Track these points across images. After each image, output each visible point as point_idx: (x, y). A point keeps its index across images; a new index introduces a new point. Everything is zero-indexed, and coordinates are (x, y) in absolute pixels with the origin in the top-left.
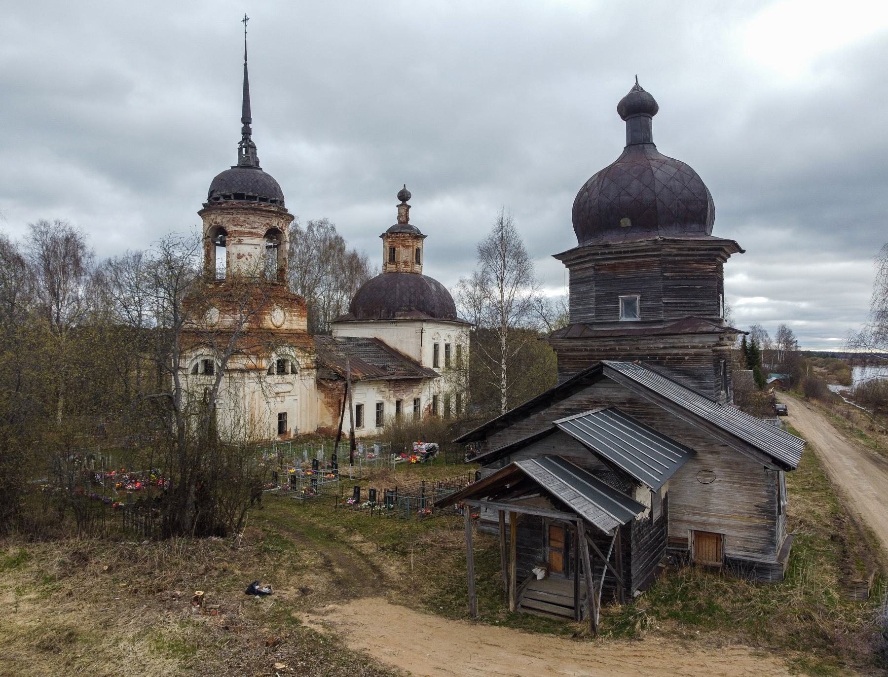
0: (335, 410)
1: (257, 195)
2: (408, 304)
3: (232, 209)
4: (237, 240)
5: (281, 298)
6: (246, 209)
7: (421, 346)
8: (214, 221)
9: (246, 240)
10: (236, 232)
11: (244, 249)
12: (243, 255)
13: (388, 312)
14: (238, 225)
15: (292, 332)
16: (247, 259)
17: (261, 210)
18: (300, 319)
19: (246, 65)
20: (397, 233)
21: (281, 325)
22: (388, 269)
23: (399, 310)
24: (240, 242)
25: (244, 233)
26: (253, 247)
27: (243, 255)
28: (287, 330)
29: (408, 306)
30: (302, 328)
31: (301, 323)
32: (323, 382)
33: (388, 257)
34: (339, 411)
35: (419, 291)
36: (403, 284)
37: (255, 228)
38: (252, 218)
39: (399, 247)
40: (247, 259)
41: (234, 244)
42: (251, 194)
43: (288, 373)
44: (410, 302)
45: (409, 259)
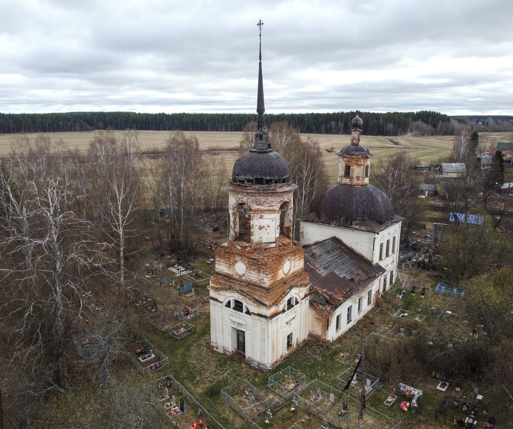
0: (323, 325)
1: (273, 178)
2: (362, 215)
3: (256, 193)
4: (259, 216)
7: (373, 250)
8: (241, 200)
9: (266, 216)
10: (258, 210)
11: (263, 222)
12: (264, 227)
13: (346, 220)
14: (260, 204)
16: (266, 229)
20: (352, 155)
21: (289, 272)
22: (343, 181)
23: (355, 220)
24: (261, 217)
25: (264, 211)
26: (271, 220)
27: (264, 227)
29: (362, 217)
30: (301, 267)
32: (315, 304)
33: (344, 172)
34: (326, 326)
35: (370, 203)
36: (358, 198)
37: (272, 206)
38: (270, 199)
39: (354, 166)
40: (266, 229)
42: (268, 178)
44: (364, 213)
45: (361, 175)
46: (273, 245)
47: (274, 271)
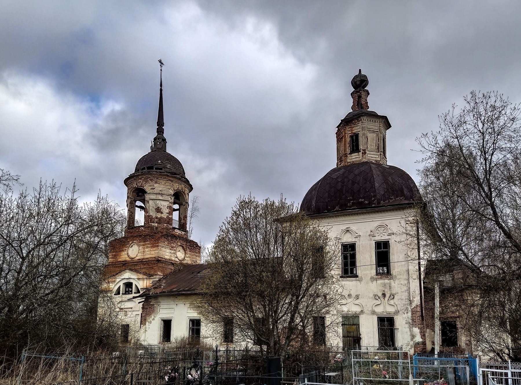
5: (135, 236)
18: (152, 249)
19: (161, 90)
28: (140, 259)
31: (153, 252)
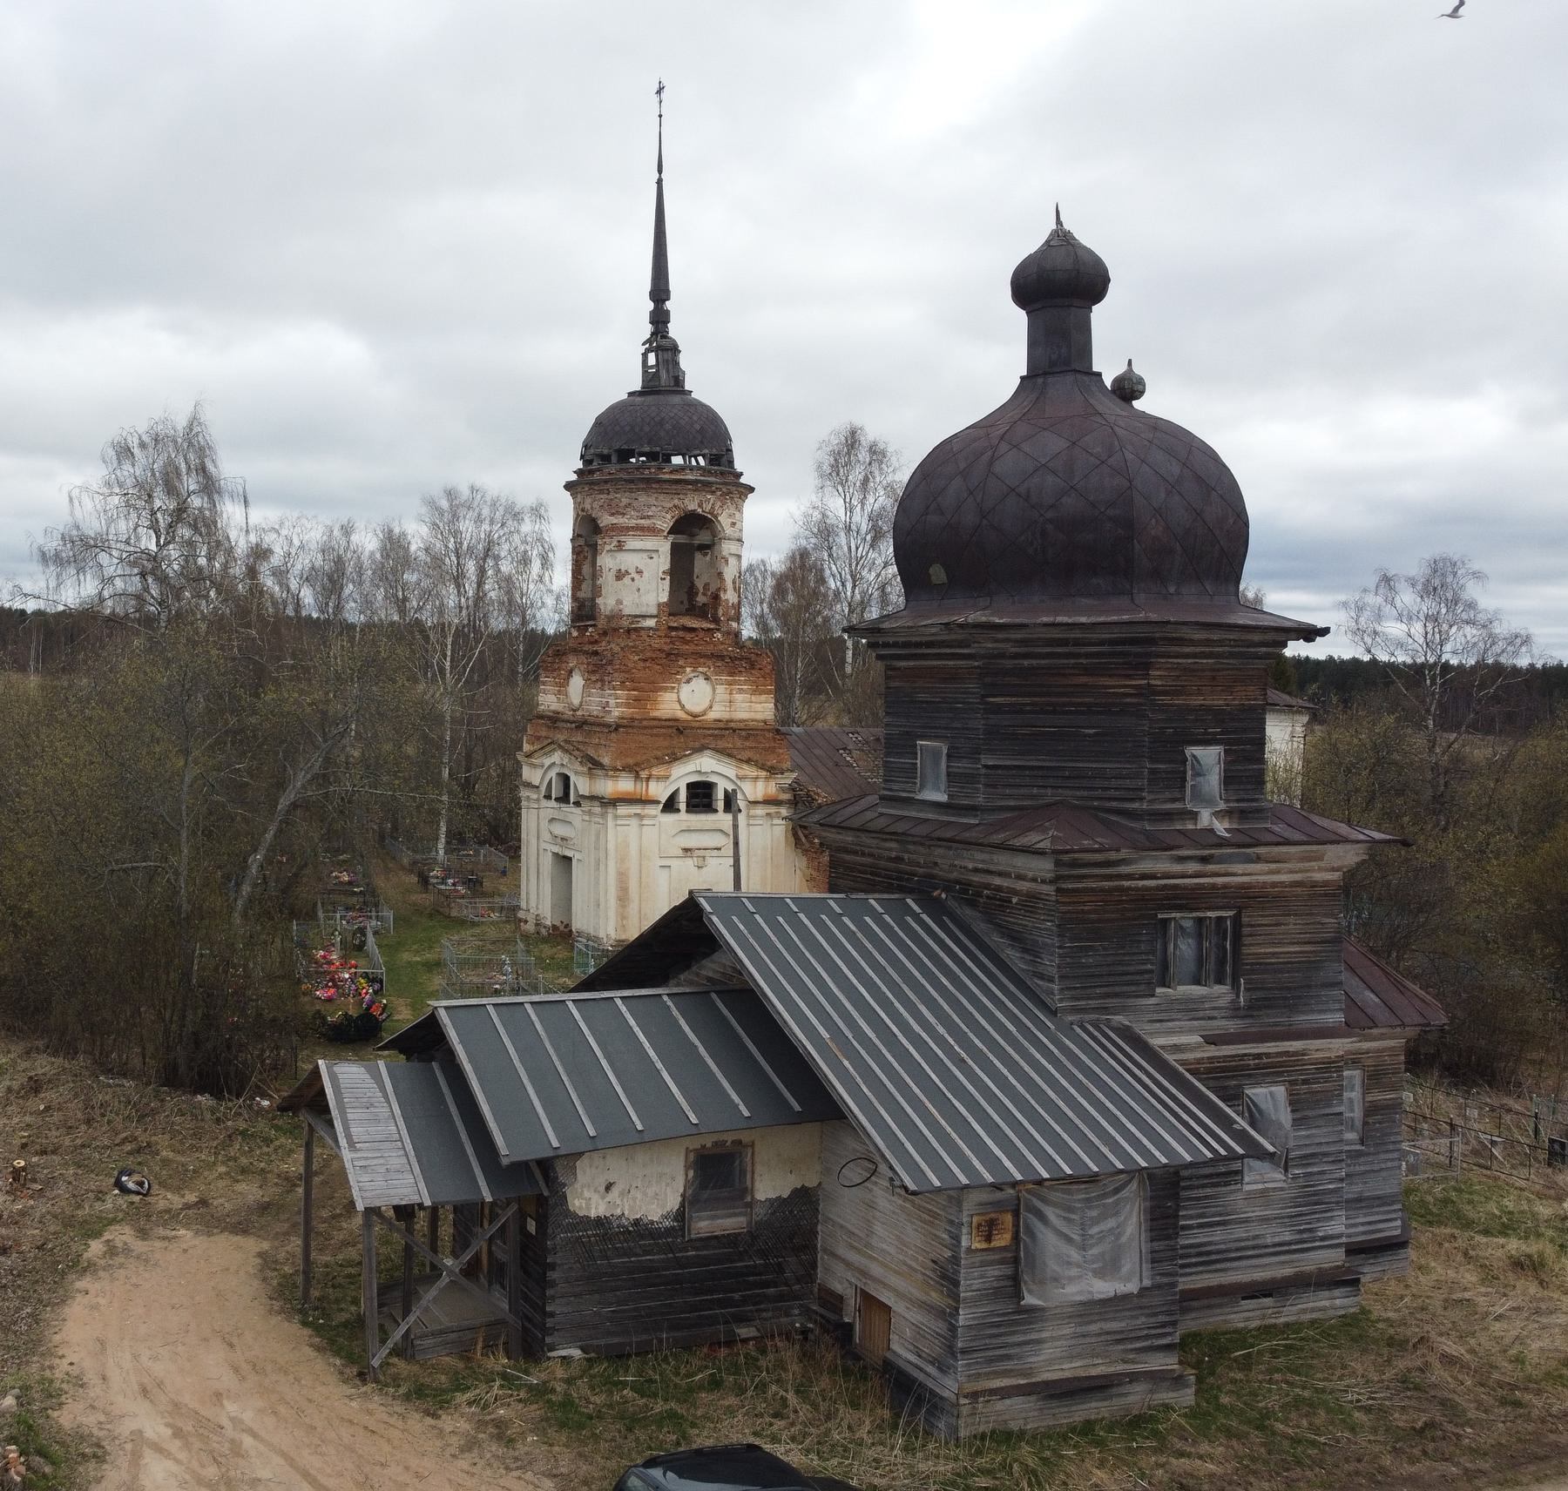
6: (631, 481)
9: (633, 543)
15: (733, 725)
17: (659, 481)
26: (645, 555)
37: (649, 517)
40: (633, 580)
41: (611, 551)
43: (716, 811)
46: (651, 623)
47: (645, 691)
